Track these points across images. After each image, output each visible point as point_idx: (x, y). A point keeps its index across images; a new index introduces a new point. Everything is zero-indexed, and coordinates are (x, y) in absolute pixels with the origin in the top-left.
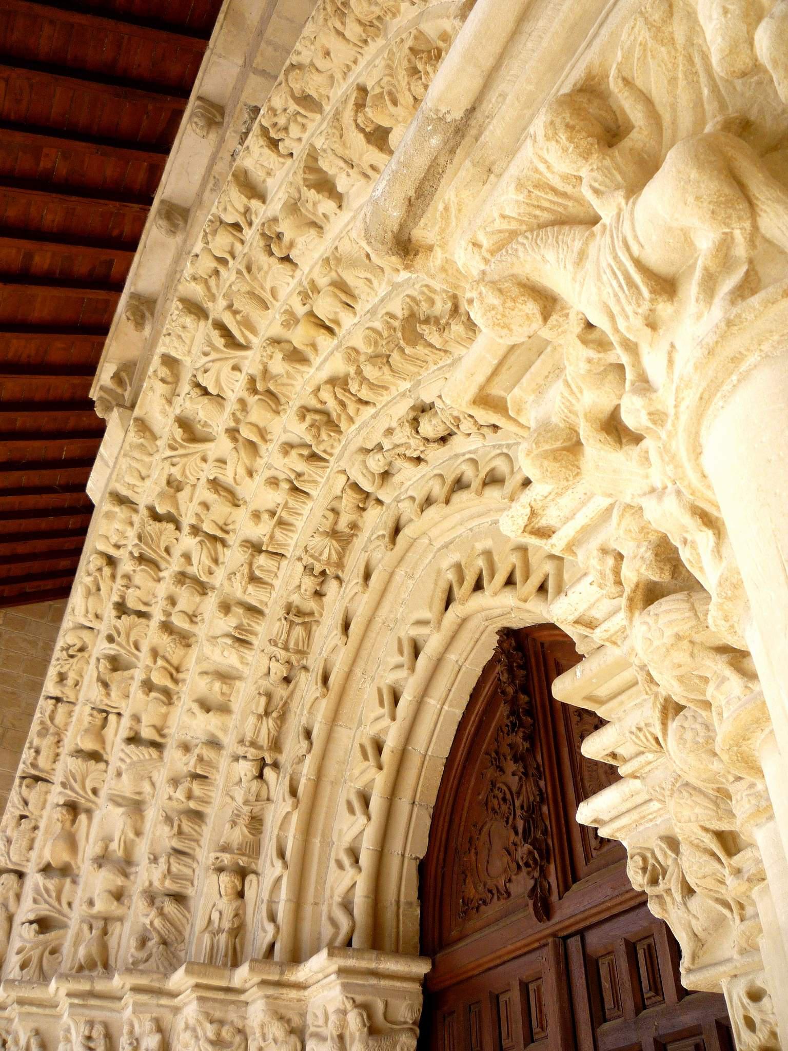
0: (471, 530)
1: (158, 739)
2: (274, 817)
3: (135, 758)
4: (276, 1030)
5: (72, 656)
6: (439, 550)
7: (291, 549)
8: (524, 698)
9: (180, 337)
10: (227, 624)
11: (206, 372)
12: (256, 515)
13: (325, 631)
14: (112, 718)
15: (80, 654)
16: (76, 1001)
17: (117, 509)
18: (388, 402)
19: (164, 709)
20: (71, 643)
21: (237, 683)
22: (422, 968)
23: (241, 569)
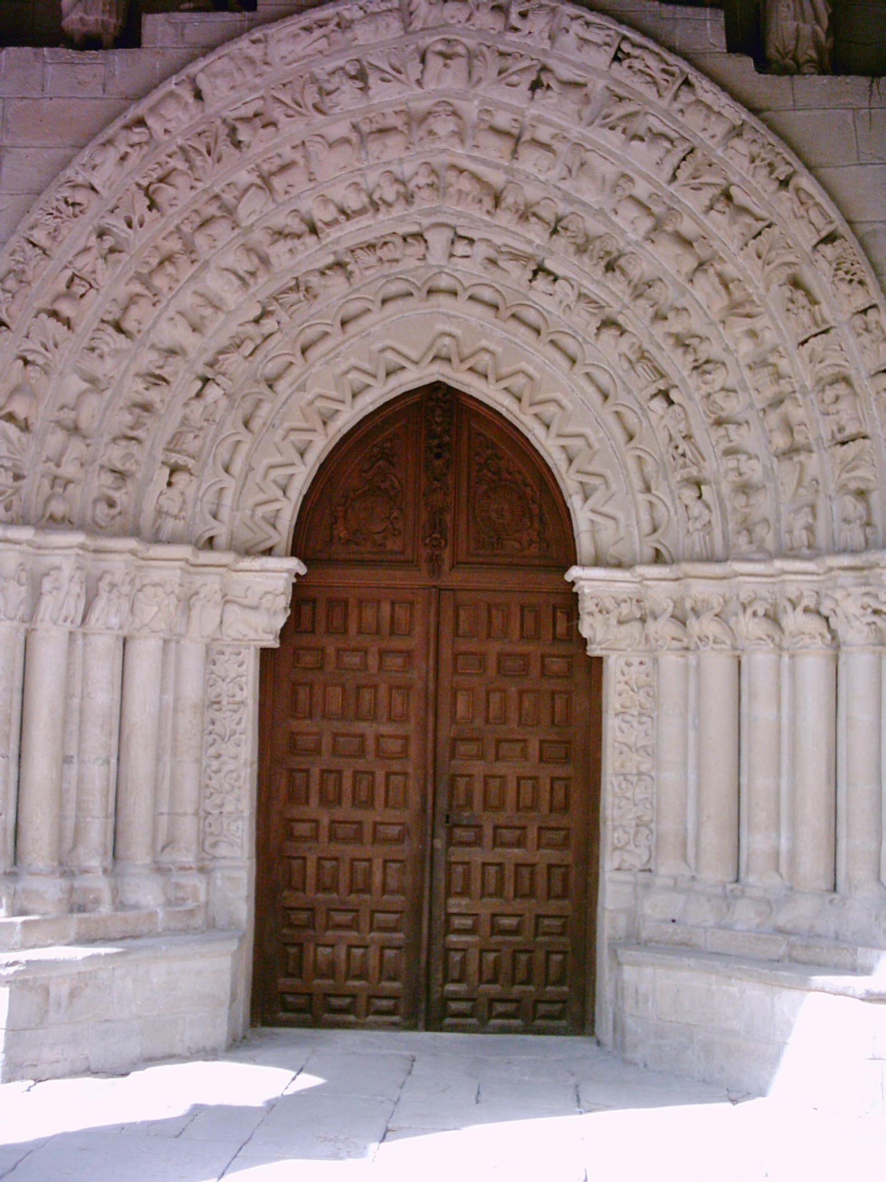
0: (482, 326)
1: (135, 332)
2: (216, 436)
3: (118, 346)
4: (218, 597)
5: (76, 216)
6: (439, 313)
7: (329, 240)
8: (447, 438)
9: (377, 28)
10: (244, 264)
11: (383, 80)
12: (325, 200)
13: (313, 311)
14: (92, 292)
15: (81, 216)
16: (81, 552)
17: (191, 100)
18: (506, 229)
19: (152, 308)
20: (78, 201)
21: (220, 313)
22: (303, 571)
23: (296, 240)
